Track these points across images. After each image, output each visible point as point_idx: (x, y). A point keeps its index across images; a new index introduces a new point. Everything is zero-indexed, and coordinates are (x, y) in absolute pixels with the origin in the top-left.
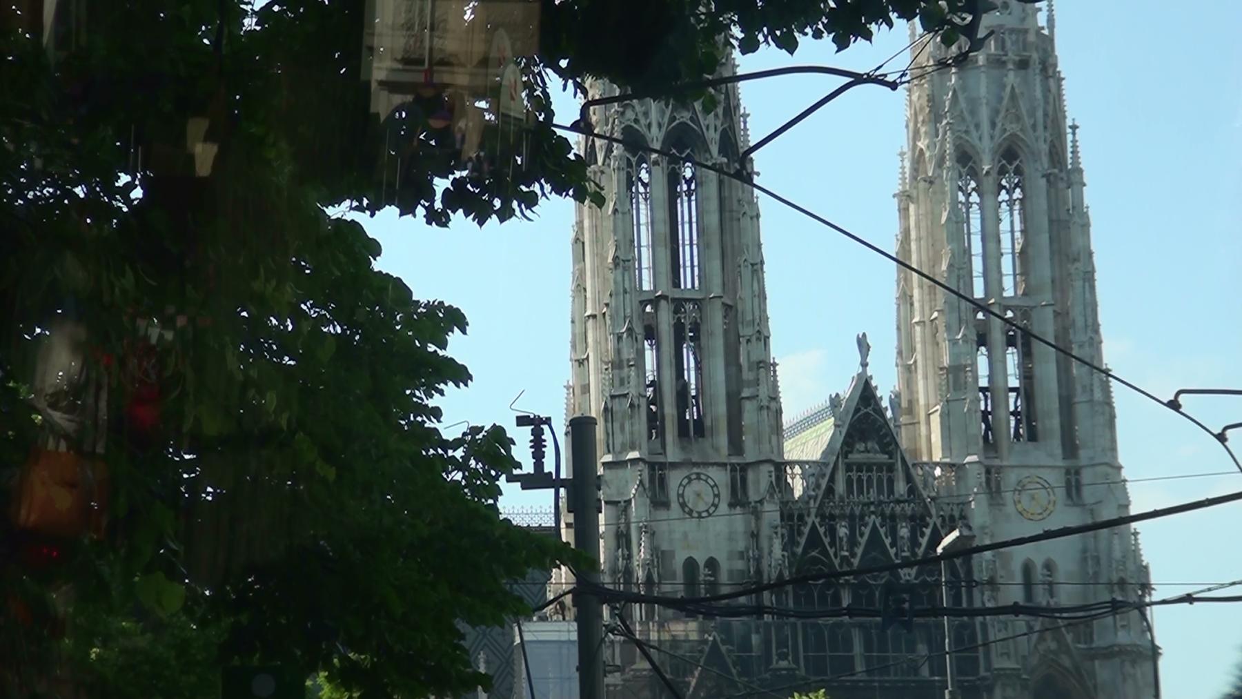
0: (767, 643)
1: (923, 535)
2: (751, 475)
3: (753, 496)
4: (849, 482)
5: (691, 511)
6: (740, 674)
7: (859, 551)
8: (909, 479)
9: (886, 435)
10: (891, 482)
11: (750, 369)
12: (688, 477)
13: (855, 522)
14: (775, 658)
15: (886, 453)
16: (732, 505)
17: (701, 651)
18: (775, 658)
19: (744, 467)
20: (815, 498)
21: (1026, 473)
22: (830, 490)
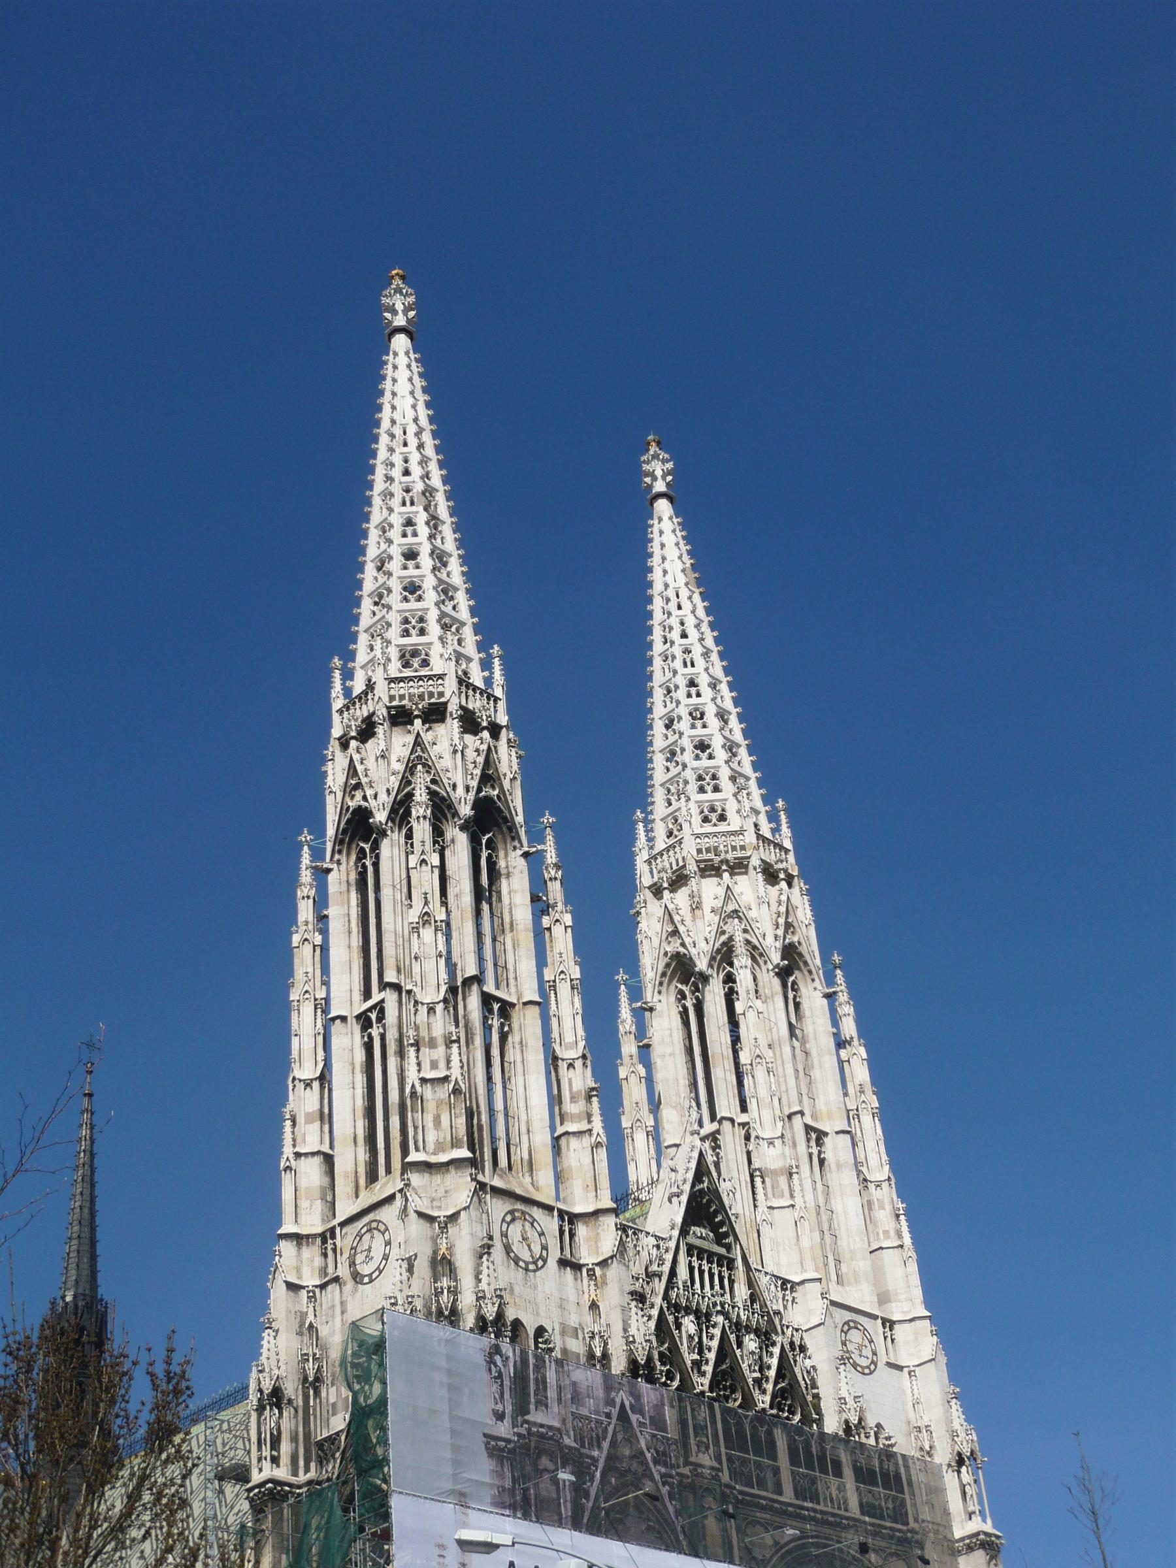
0: (683, 1422)
1: (772, 1355)
2: (582, 1230)
3: (587, 1257)
4: (691, 1269)
5: (516, 1260)
6: (656, 1462)
7: (712, 1356)
8: (751, 1284)
9: (722, 1224)
10: (732, 1282)
11: (573, 1099)
12: (512, 1212)
13: (703, 1318)
14: (694, 1448)
15: (719, 1243)
16: (563, 1263)
17: (608, 1415)
18: (694, 1448)
19: (573, 1218)
20: (660, 1276)
21: (848, 1316)
22: (673, 1273)
